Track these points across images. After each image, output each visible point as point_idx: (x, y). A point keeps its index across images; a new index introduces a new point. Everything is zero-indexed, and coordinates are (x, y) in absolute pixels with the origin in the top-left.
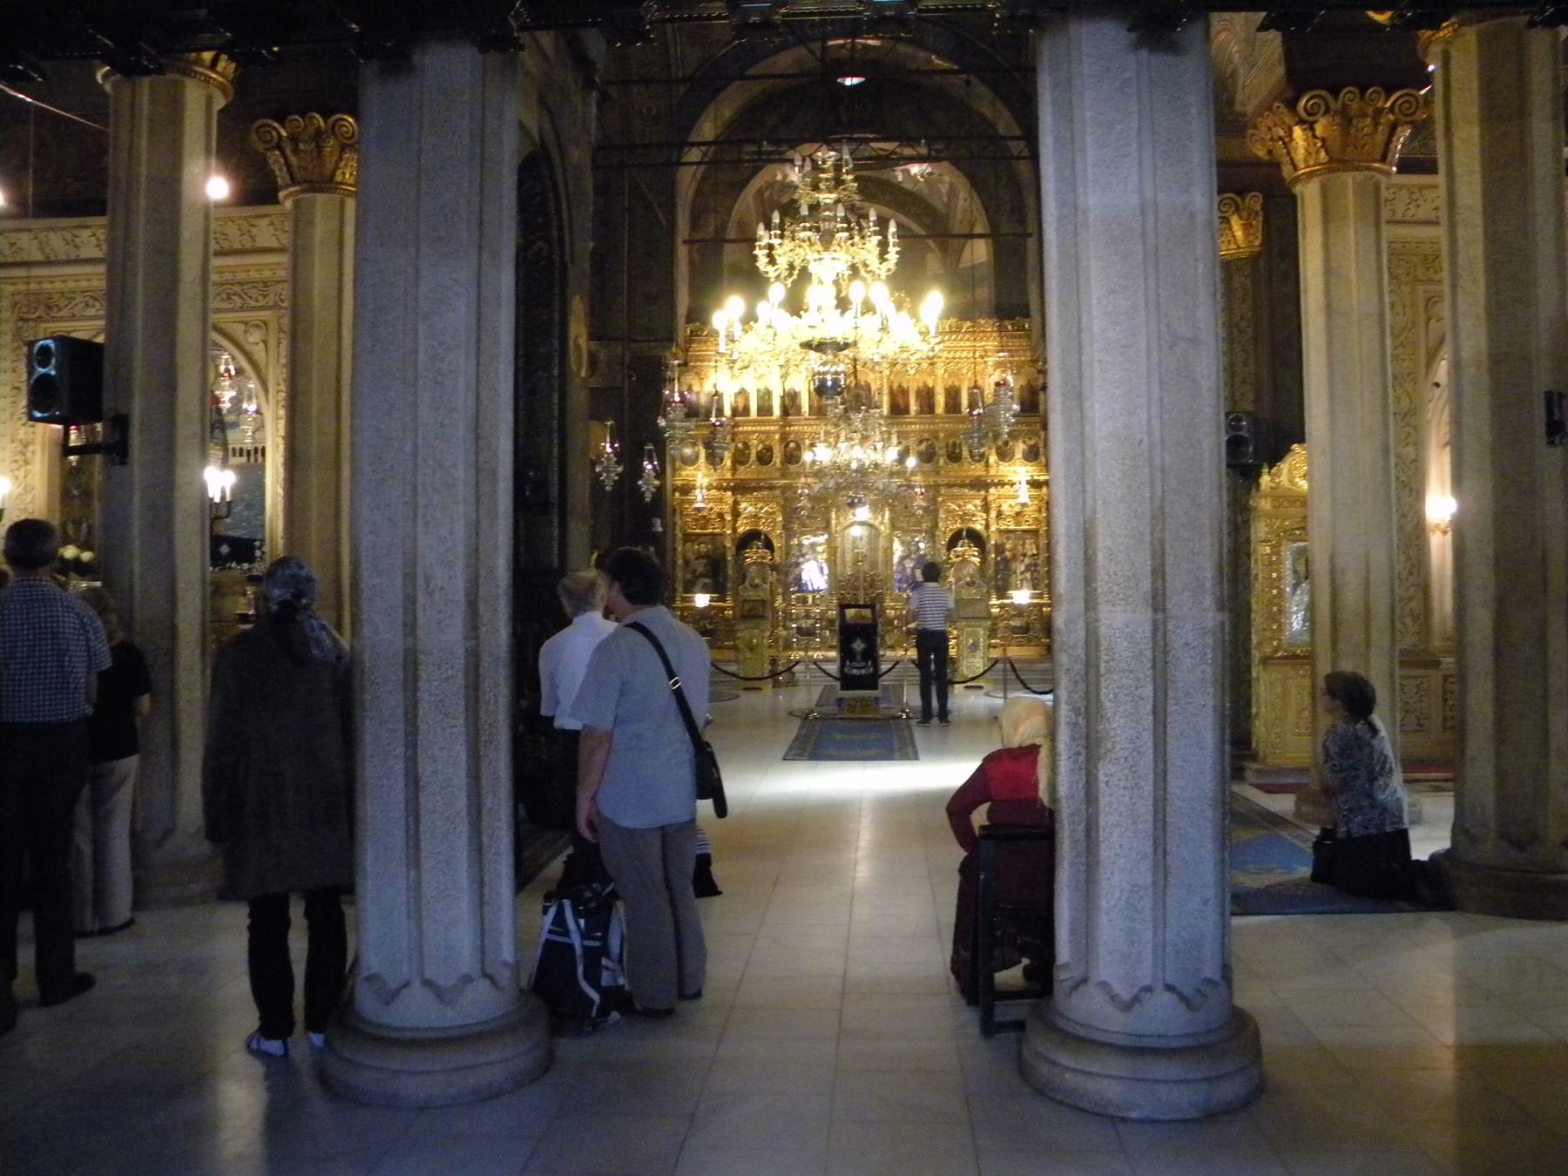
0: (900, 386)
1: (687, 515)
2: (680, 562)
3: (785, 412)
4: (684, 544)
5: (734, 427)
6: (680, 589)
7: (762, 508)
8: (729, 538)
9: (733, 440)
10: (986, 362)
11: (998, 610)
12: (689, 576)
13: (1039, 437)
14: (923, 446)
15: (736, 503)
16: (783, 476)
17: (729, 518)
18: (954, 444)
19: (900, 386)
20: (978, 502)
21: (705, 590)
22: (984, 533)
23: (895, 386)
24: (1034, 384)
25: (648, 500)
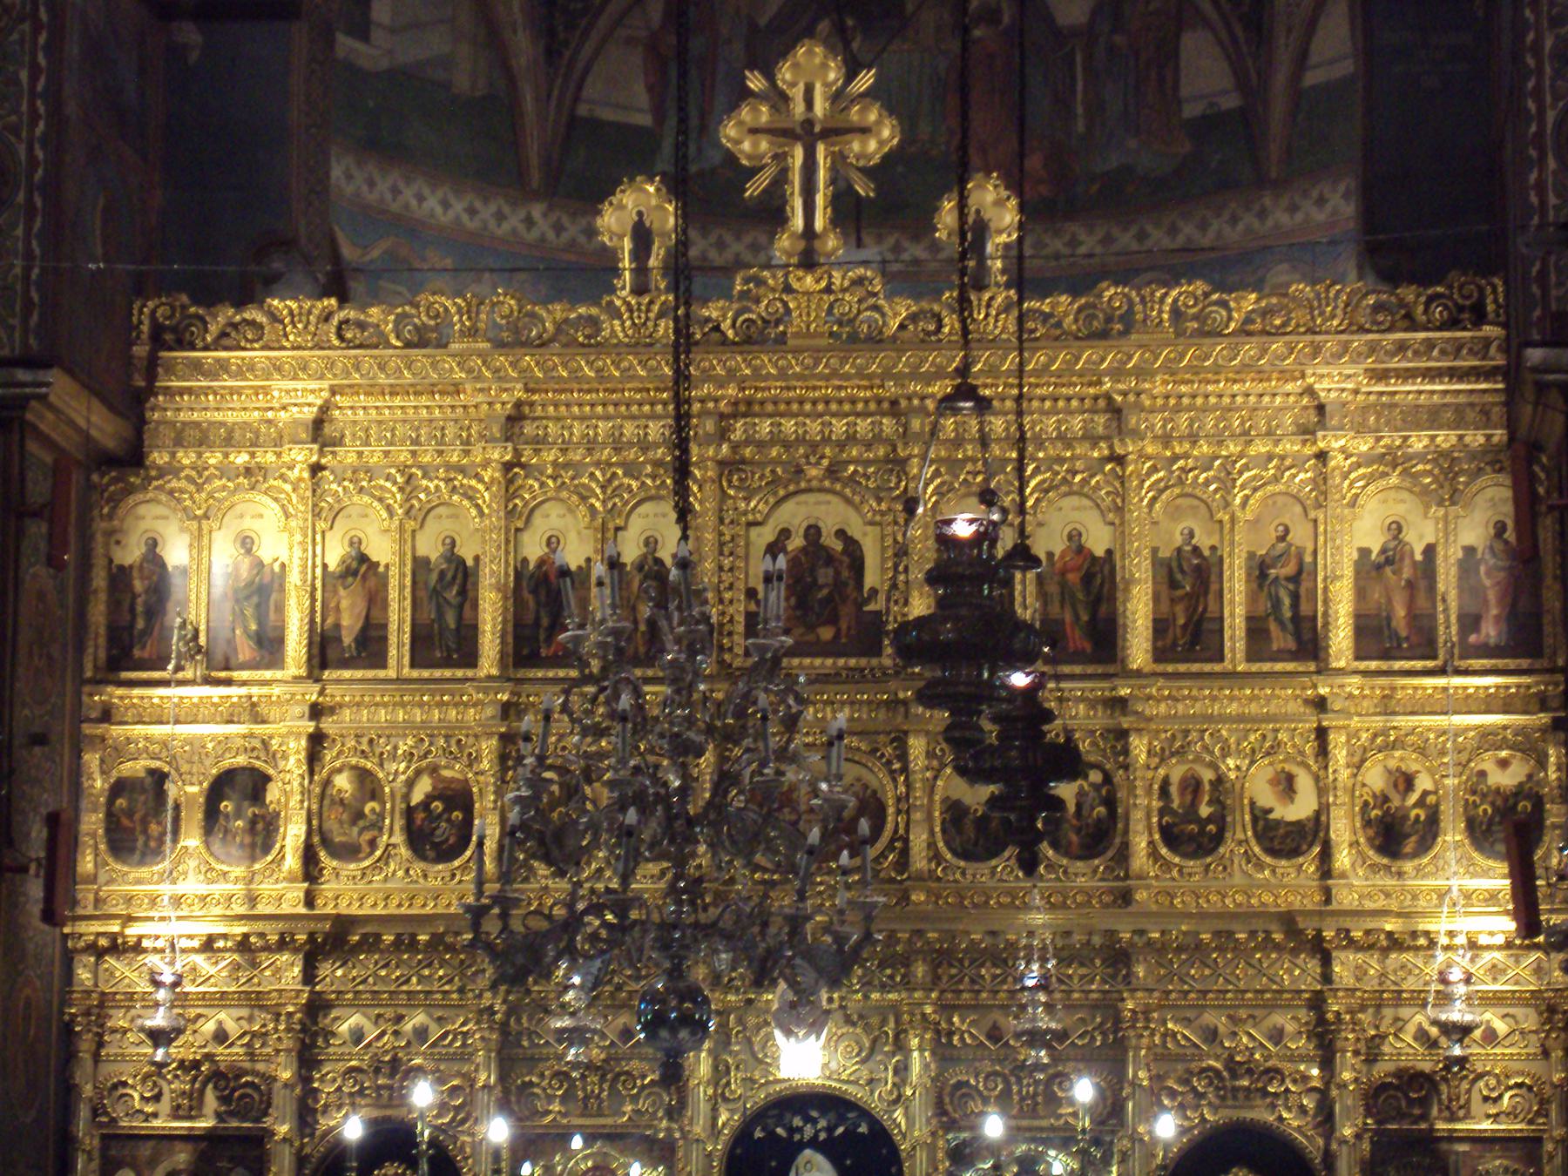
10: (1322, 456)
17: (286, 1075)
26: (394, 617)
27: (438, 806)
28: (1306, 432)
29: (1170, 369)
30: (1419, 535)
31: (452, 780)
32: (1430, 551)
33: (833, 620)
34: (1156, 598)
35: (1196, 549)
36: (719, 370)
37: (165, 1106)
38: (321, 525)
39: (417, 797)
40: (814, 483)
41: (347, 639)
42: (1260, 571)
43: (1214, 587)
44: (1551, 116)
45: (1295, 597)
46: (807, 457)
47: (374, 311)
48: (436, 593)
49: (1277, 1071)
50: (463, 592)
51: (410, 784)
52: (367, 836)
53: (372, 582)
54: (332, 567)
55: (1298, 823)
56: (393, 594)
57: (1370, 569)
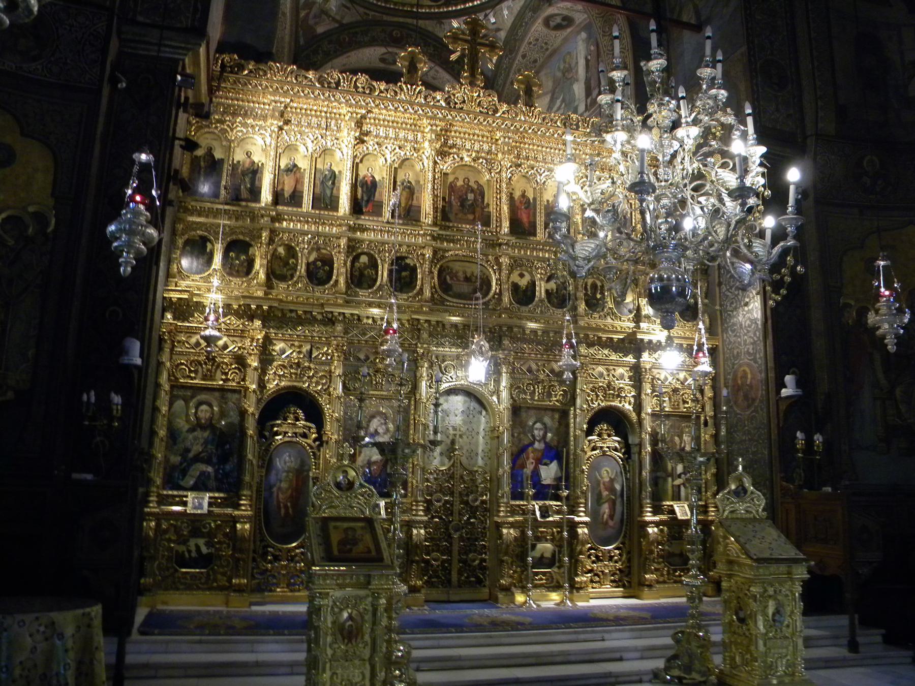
0: (523, 195)
1: (181, 353)
2: (162, 433)
3: (357, 208)
4: (171, 404)
5: (274, 220)
6: (159, 481)
8: (253, 398)
9: (271, 241)
11: (656, 530)
12: (175, 459)
14: (552, 285)
16: (347, 303)
17: (255, 364)
18: (594, 286)
19: (523, 195)
21: (200, 486)
22: (634, 416)
23: (517, 194)
25: (125, 270)
26: (306, 188)
27: (319, 263)
31: (325, 254)
33: (474, 213)
36: (440, 115)
37: (200, 375)
38: (280, 151)
39: (312, 259)
40: (468, 163)
41: (287, 195)
46: (468, 150)
50: (333, 183)
51: (309, 253)
52: (290, 272)
53: (298, 175)
54: (282, 167)
56: (306, 180)
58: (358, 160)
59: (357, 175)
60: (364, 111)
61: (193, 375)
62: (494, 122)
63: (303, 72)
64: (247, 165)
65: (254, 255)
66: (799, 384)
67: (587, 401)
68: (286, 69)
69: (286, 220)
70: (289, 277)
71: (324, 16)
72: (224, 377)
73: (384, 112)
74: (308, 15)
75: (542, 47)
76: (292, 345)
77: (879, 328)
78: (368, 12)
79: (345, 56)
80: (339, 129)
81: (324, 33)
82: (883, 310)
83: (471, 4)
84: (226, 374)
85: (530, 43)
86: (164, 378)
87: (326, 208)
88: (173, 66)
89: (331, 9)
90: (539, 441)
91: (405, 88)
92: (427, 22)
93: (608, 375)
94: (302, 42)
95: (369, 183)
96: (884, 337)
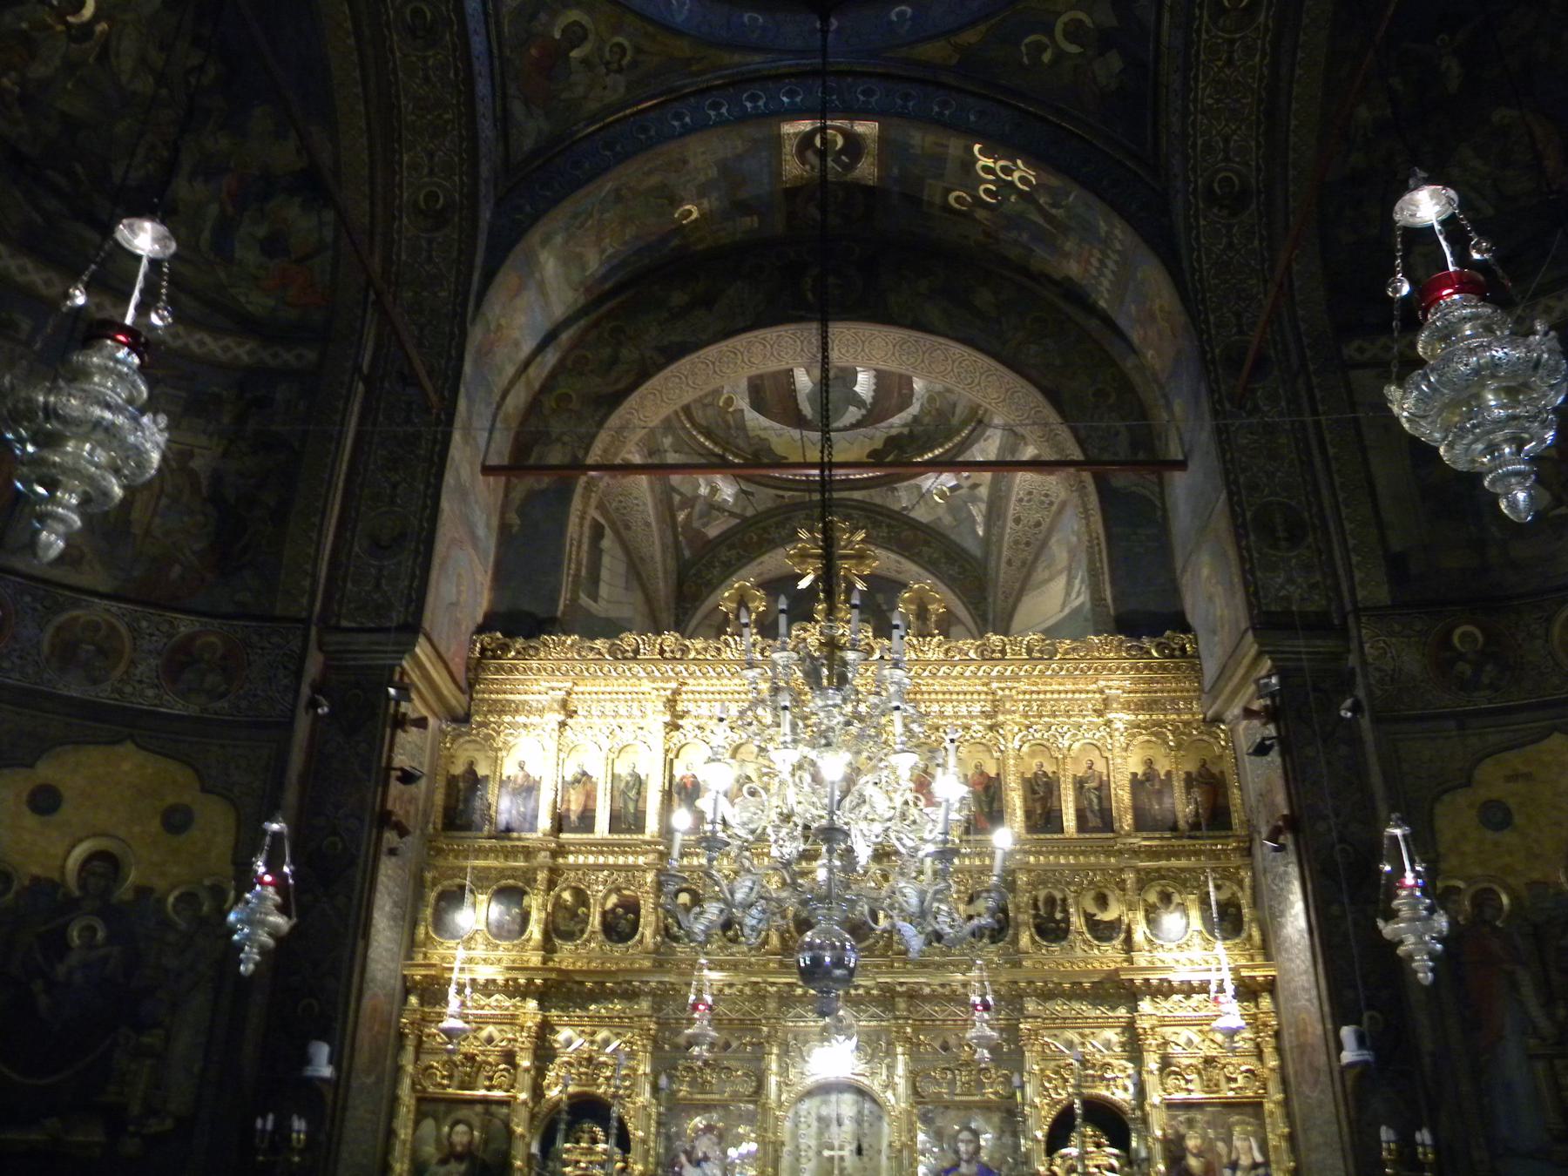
1: (433, 1052)
4: (417, 1123)
5: (555, 854)
7: (606, 1042)
8: (524, 1114)
9: (551, 884)
13: (1240, 883)
15: (546, 1028)
18: (1051, 901)
20: (1112, 1035)
24: (1215, 770)
27: (620, 911)
28: (1100, 713)
29: (1029, 675)
30: (1162, 767)
32: (1168, 774)
34: (1025, 800)
35: (1045, 774)
37: (456, 1082)
39: (609, 904)
41: (573, 817)
42: (1080, 785)
43: (1056, 793)
44: (1249, 515)
45: (1100, 798)
47: (598, 642)
48: (624, 793)
49: (1109, 1064)
50: (639, 793)
51: (606, 898)
53: (588, 786)
55: (1111, 922)
57: (1137, 784)
58: (671, 756)
59: (672, 777)
60: (674, 685)
61: (445, 1082)
62: (867, 670)
63: (588, 644)
64: (520, 781)
65: (530, 906)
66: (1361, 1041)
67: (1046, 1089)
68: (565, 642)
69: (572, 853)
70: (578, 934)
71: (715, 513)
72: (487, 1083)
73: (703, 681)
74: (689, 516)
75: (1042, 502)
76: (583, 1032)
77: (1401, 942)
78: (781, 493)
79: (755, 563)
80: (643, 714)
81: (719, 536)
82: (1405, 912)
83: (930, 455)
84: (491, 1078)
85: (1021, 500)
86: (405, 1091)
87: (629, 831)
88: (386, 675)
89: (725, 500)
90: (968, 1162)
91: (732, 643)
92: (873, 491)
93: (1083, 1044)
94: (687, 553)
95: (689, 786)
96: (1410, 957)
